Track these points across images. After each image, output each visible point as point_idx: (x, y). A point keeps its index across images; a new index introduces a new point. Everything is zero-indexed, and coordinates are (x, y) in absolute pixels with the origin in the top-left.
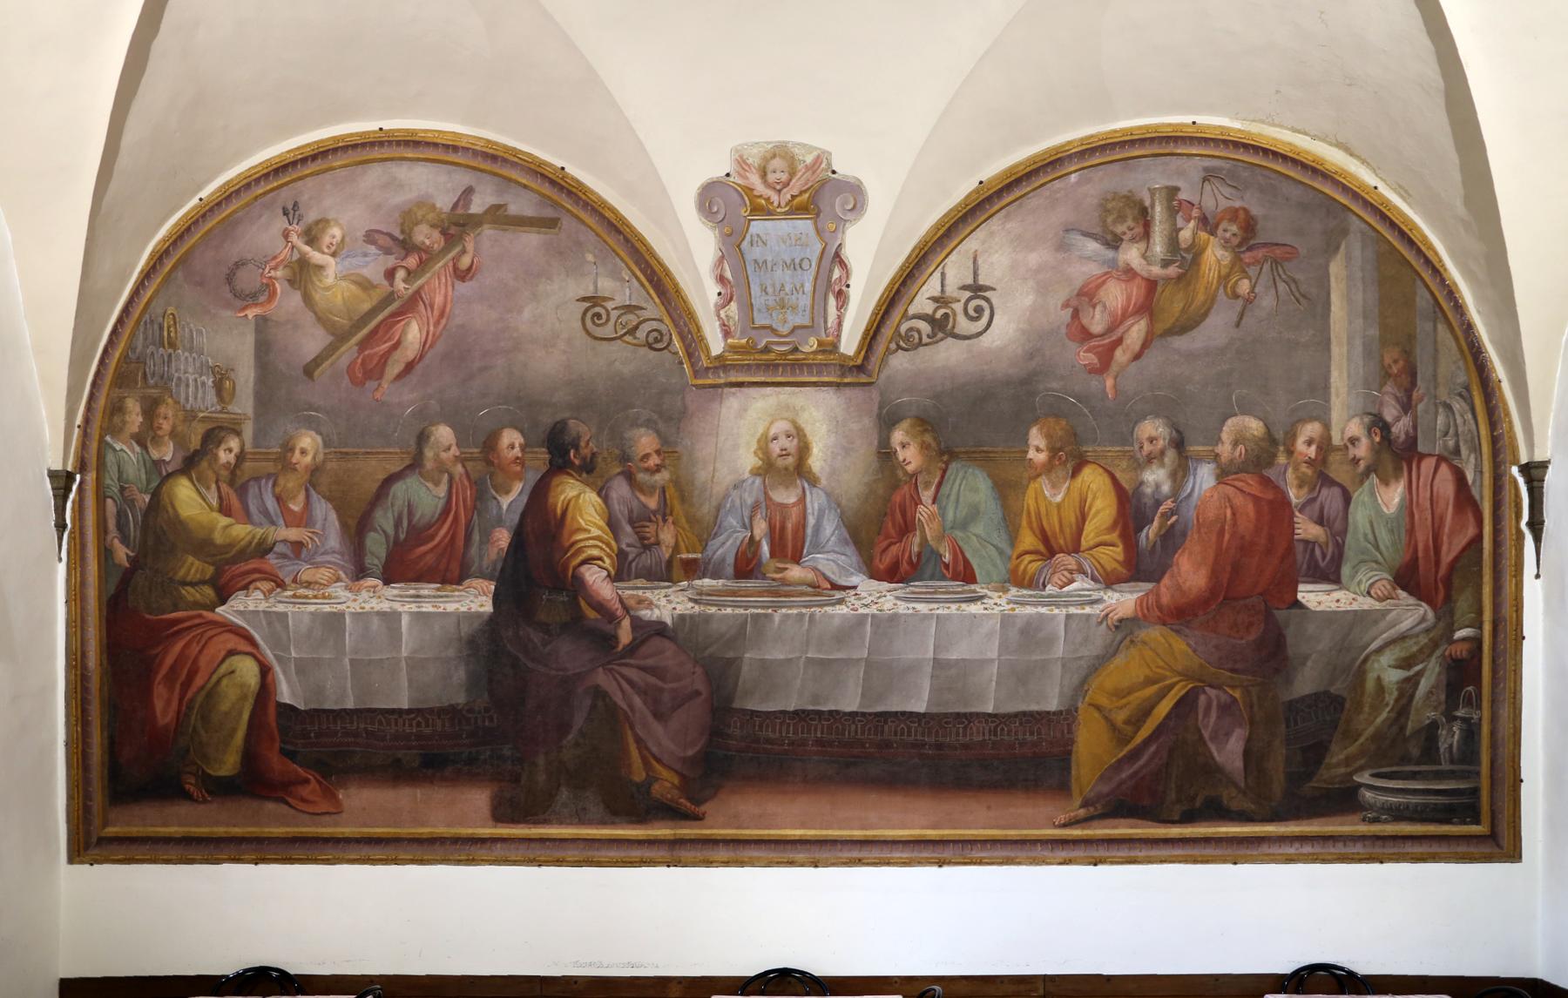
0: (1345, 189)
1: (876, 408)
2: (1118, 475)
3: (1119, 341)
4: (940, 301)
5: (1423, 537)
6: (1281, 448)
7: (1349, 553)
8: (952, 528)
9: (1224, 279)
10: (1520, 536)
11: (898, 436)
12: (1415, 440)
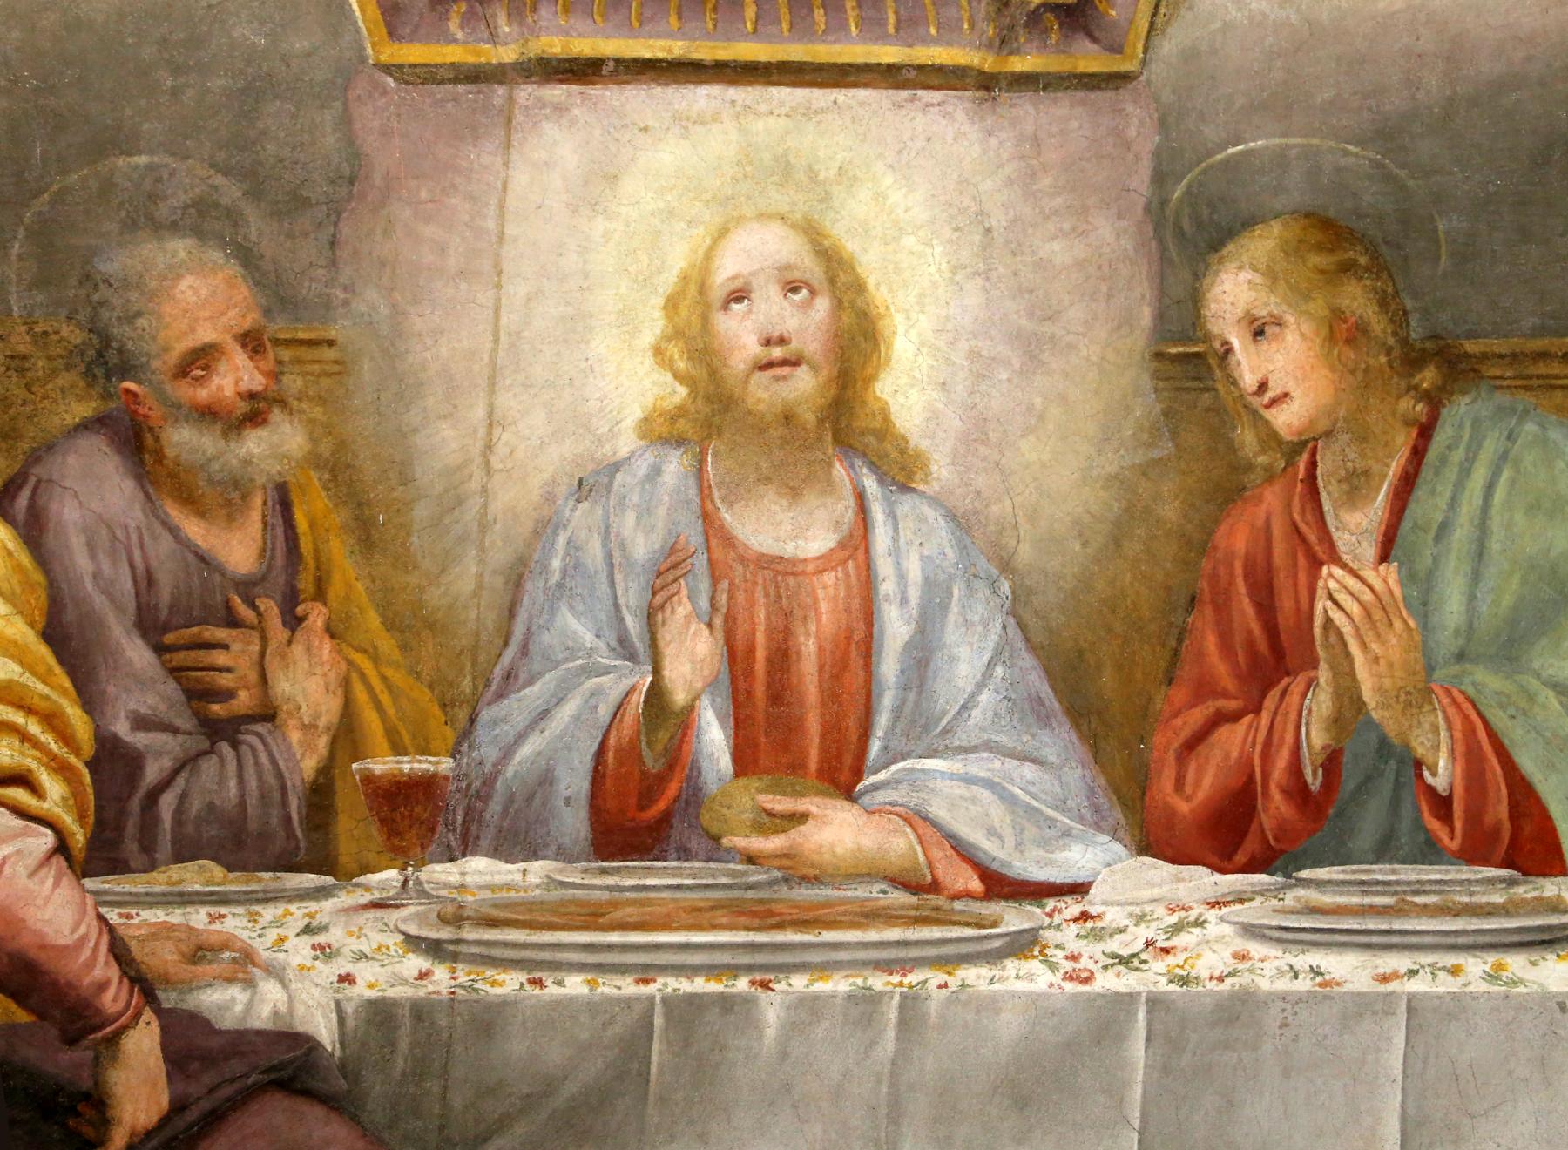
1: (1141, 181)
8: (1461, 657)
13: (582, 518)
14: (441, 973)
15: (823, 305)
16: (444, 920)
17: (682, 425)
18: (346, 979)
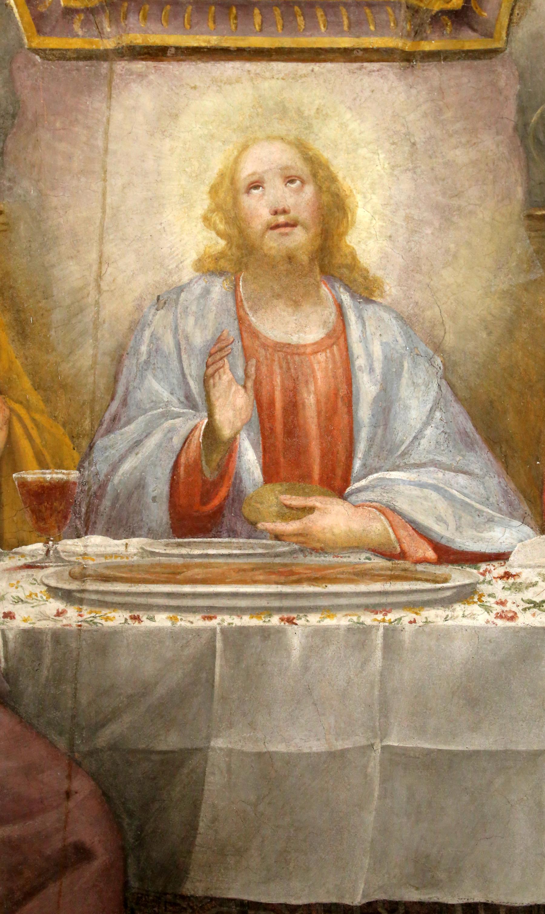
14: (72, 612)
15: (309, 190)
16: (73, 577)
17: (222, 263)
18: (9, 615)
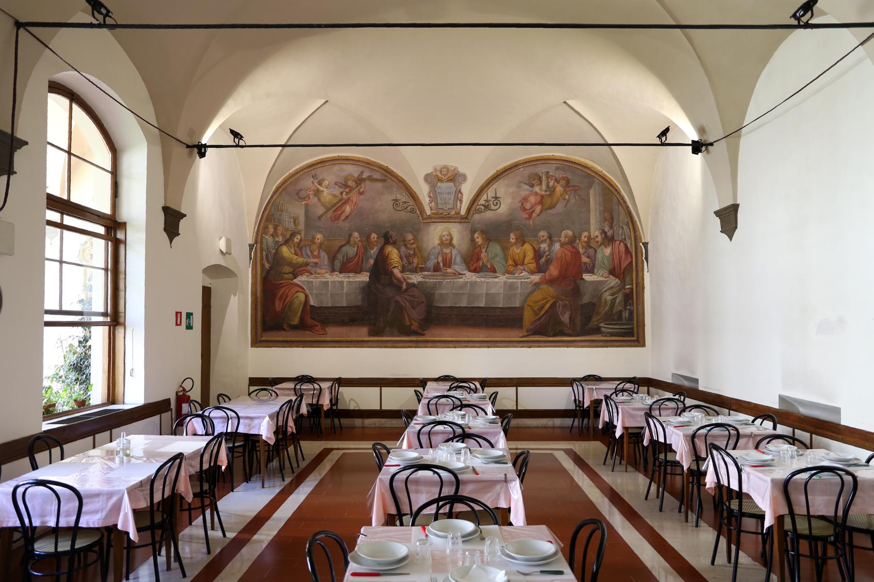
0: (594, 172)
1: (470, 229)
2: (534, 245)
3: (534, 211)
4: (487, 201)
5: (616, 261)
6: (578, 239)
7: (597, 265)
9: (562, 195)
10: (643, 261)
11: (476, 235)
12: (614, 236)
13: (433, 250)
